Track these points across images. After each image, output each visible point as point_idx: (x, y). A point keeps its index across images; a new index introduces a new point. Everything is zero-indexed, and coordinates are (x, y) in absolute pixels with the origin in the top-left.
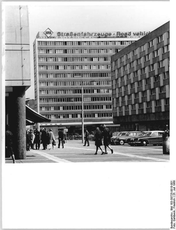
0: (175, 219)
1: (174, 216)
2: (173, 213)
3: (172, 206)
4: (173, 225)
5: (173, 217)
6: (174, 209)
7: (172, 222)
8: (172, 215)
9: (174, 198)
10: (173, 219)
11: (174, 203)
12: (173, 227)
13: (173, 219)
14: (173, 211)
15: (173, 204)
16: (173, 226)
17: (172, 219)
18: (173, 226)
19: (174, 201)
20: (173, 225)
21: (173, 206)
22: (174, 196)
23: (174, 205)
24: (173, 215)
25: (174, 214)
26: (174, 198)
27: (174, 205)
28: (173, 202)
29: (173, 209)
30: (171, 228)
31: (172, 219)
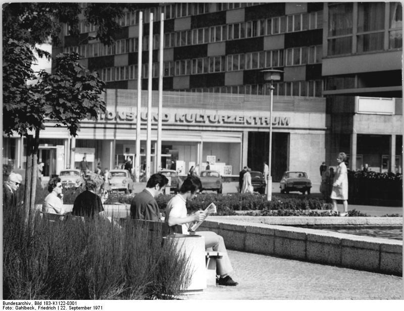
0: (20, 309)
1: (25, 308)
3: (43, 303)
4: (10, 306)
5: (23, 306)
6: (36, 307)
7: (14, 303)
8: (27, 304)
11: (48, 308)
12: (5, 305)
14: (34, 306)
15: (46, 306)
16: (7, 306)
17: (20, 304)
19: (51, 308)
20: (10, 306)
21: (41, 306)
22: (60, 308)
23: (44, 308)
24: (27, 306)
25: (28, 308)
27: (44, 308)
28: (49, 306)
30: (4, 303)
31: (20, 304)
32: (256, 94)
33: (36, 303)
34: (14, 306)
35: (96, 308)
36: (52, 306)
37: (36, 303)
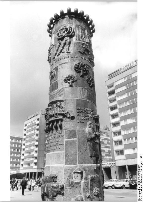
0: (142, 192)
1: (142, 190)
2: (140, 188)
3: (139, 181)
4: (140, 197)
5: (141, 191)
6: (141, 184)
7: (139, 195)
8: (140, 188)
9: (141, 174)
10: (140, 192)
11: (142, 178)
12: (140, 199)
13: (140, 192)
14: (140, 185)
15: (141, 179)
16: (140, 198)
17: (139, 192)
18: (140, 198)
19: (142, 177)
20: (140, 197)
21: (140, 181)
22: (141, 172)
23: (142, 180)
24: (141, 189)
25: (142, 188)
26: (141, 174)
27: (142, 180)
28: (141, 178)
29: (140, 183)
30: (139, 200)
31: (139, 192)
32: (34, 172)
33: (139, 184)
34: (141, 195)
35: (141, 157)
36: (140, 176)
37: (139, 184)
